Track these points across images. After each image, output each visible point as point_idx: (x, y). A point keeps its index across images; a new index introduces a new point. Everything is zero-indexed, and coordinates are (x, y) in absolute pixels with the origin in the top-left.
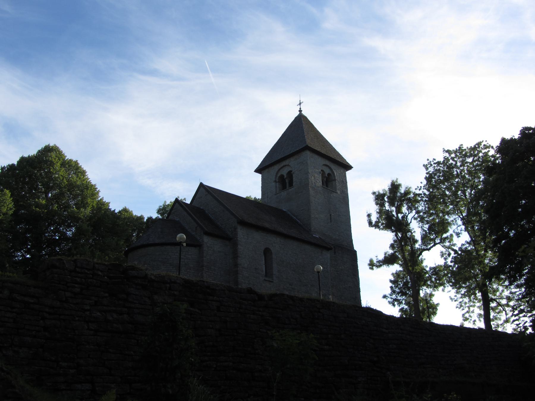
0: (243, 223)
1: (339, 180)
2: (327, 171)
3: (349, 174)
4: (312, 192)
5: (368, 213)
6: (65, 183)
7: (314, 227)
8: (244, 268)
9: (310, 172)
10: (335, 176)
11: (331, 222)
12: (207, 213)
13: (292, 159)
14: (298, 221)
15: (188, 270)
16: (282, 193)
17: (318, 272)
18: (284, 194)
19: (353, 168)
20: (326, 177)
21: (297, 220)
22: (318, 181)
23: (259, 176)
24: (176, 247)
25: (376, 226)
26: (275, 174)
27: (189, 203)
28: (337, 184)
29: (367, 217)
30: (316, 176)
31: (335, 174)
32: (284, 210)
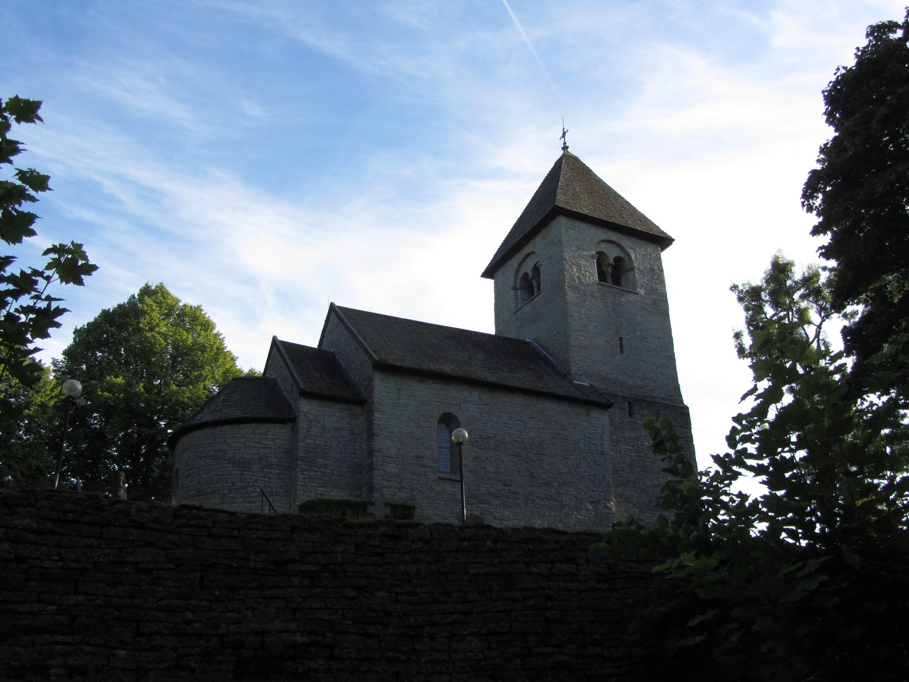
0: (383, 367)
1: (642, 268)
2: (612, 253)
3: (667, 256)
4: (571, 296)
5: (736, 331)
6: (161, 344)
7: (578, 366)
8: (389, 457)
9: (566, 257)
10: (632, 262)
11: (622, 352)
12: (338, 358)
13: (538, 239)
14: (550, 357)
15: (267, 470)
16: (524, 307)
17: (460, 444)
18: (528, 309)
19: (673, 240)
20: (610, 265)
21: (548, 356)
22: (587, 273)
23: (490, 283)
24: (241, 426)
26: (514, 275)
27: (316, 347)
28: (636, 275)
29: (734, 340)
30: (584, 263)
31: (633, 256)
32: (528, 340)
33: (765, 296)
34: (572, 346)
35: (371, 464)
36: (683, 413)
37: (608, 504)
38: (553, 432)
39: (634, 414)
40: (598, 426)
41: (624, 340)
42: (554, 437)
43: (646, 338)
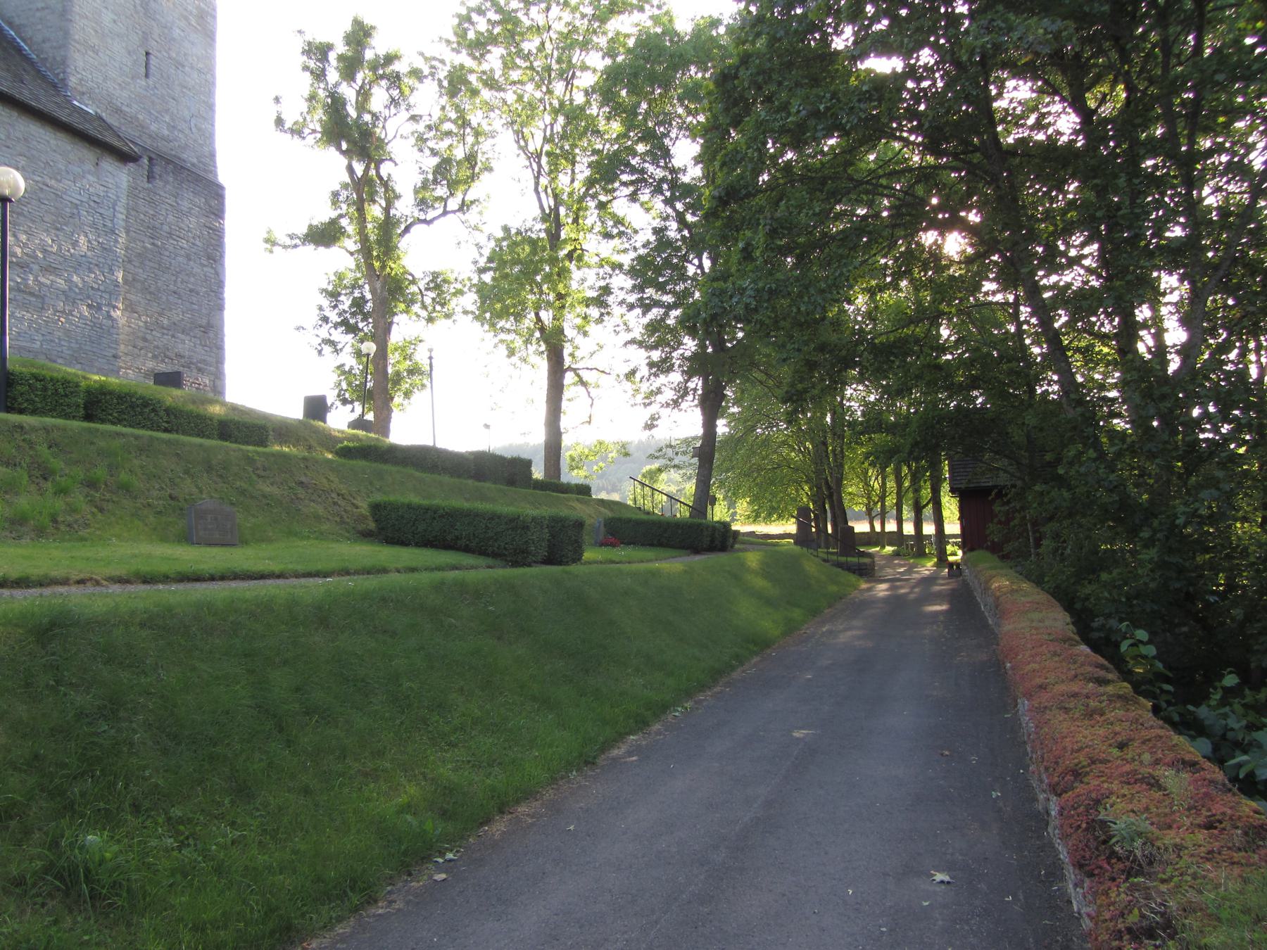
11: (147, 76)
21: (19, 40)
25: (297, 131)
33: (332, 56)
34: (75, 41)
36: (213, 196)
37: (112, 313)
38: (39, 179)
39: (154, 178)
40: (110, 186)
41: (152, 57)
42: (42, 189)
43: (183, 66)
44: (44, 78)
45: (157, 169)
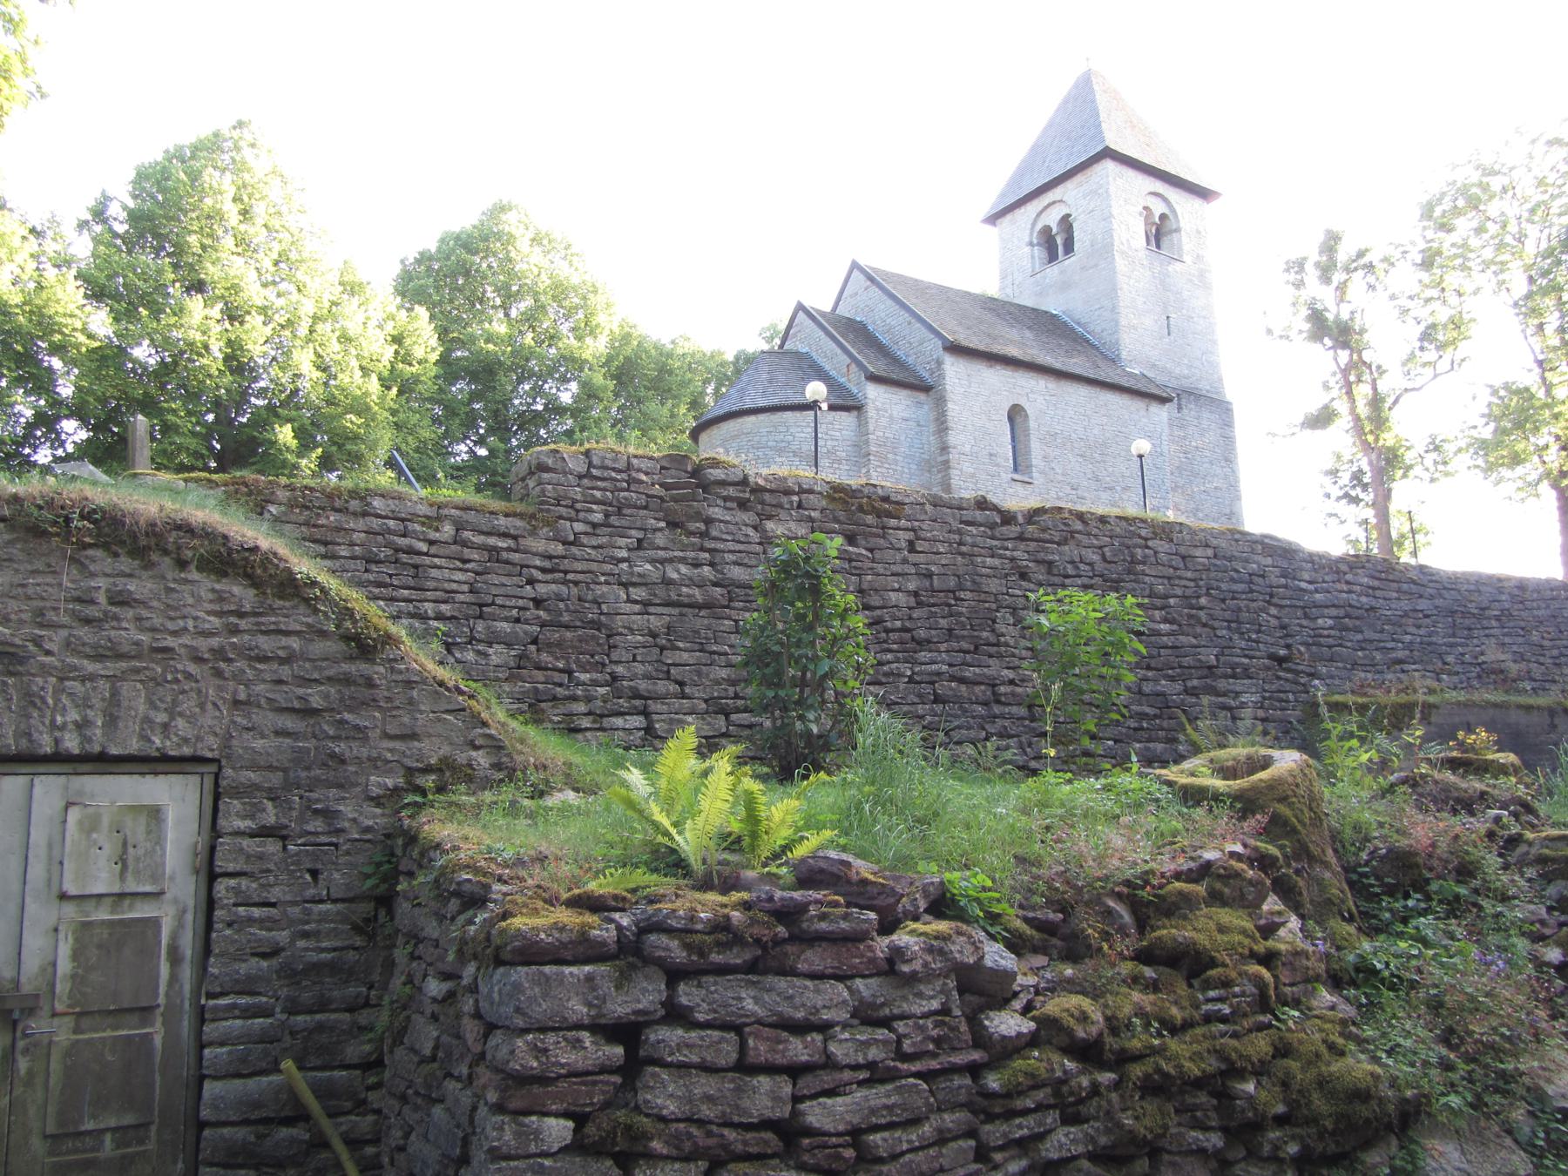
0: (956, 349)
2: (1158, 208)
4: (1121, 264)
13: (1070, 185)
17: (1141, 456)
18: (1053, 271)
35: (947, 462)
36: (1222, 409)
44: (1106, 357)
45: (1183, 402)
